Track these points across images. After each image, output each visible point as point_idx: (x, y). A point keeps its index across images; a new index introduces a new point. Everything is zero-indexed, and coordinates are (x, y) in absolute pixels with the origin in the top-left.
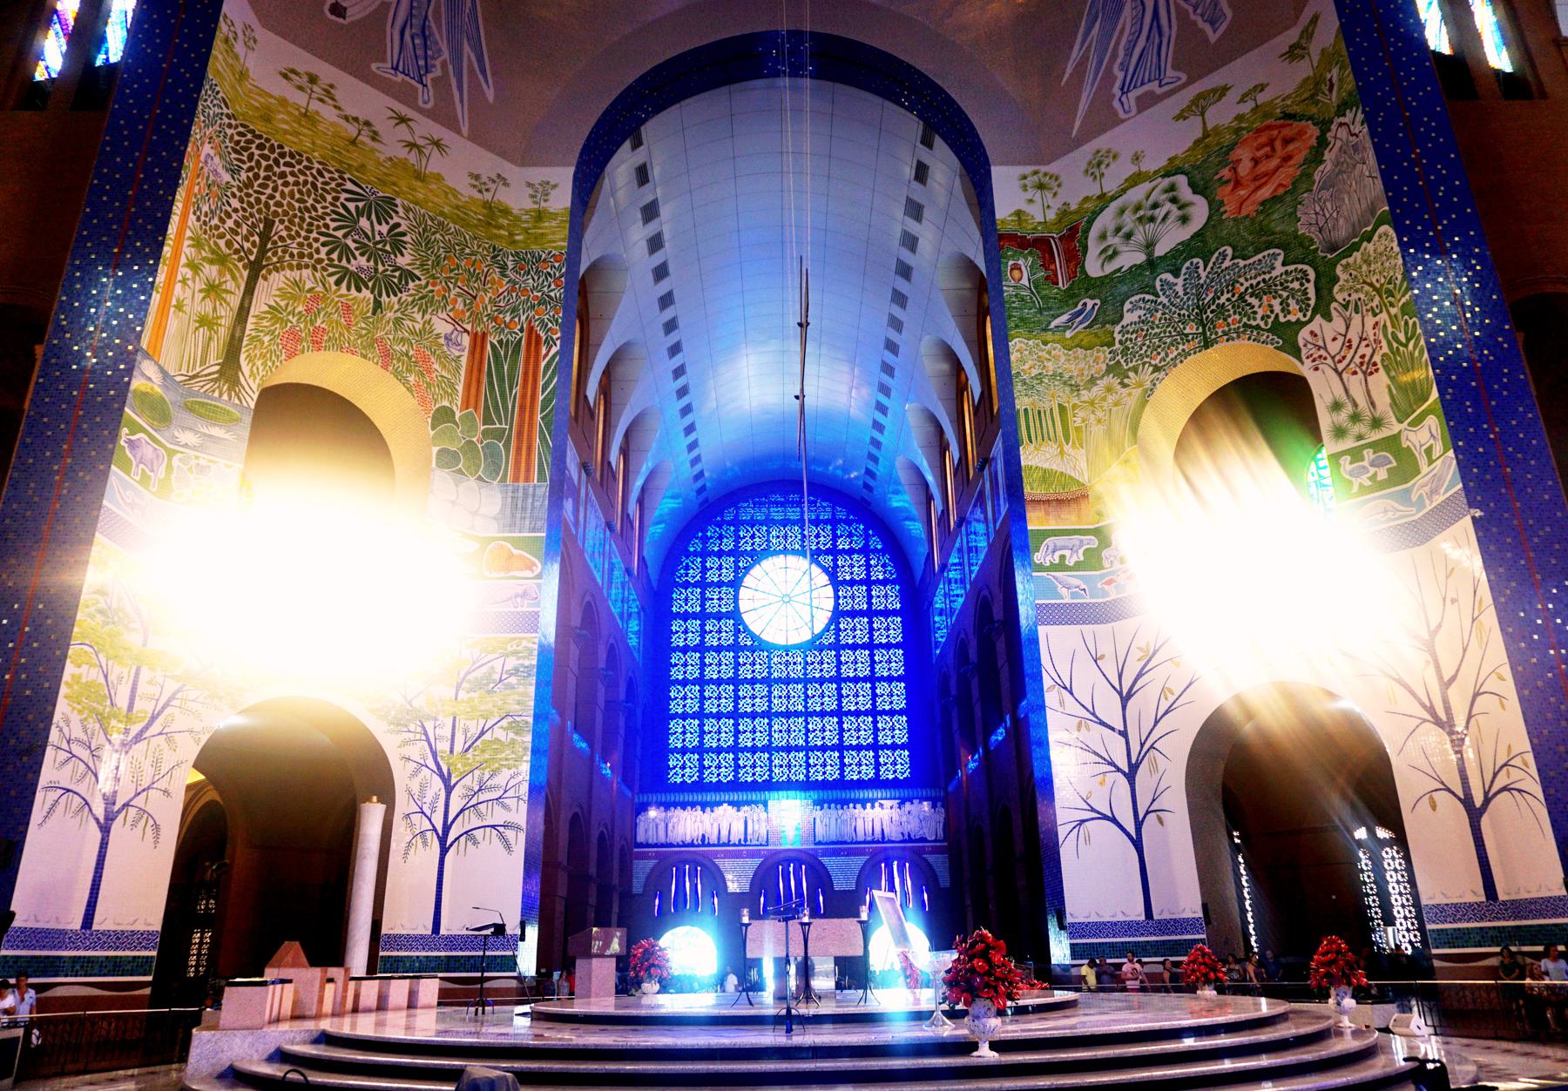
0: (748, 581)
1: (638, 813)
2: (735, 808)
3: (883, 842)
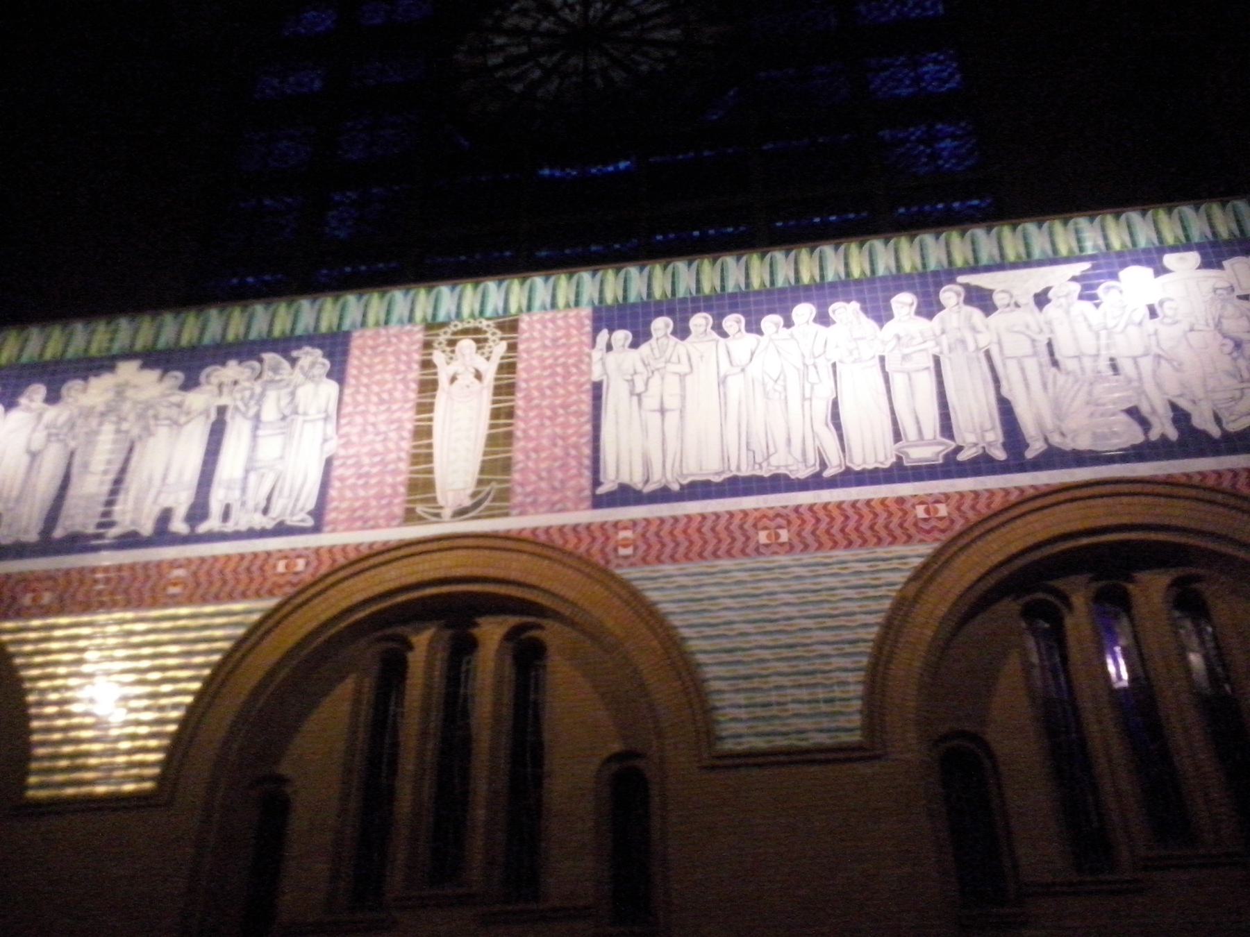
2: (178, 376)
3: (1017, 460)
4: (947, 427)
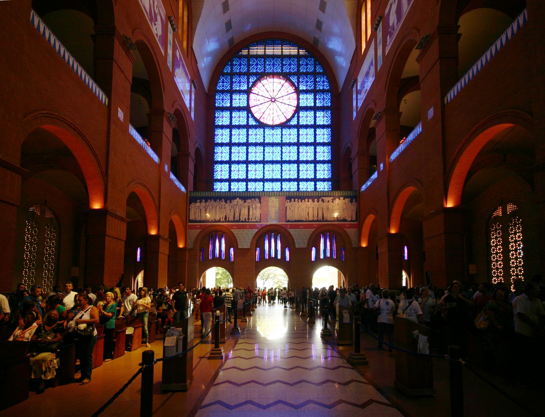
0: (255, 90)
1: (190, 204)
2: (243, 201)
4: (318, 217)
